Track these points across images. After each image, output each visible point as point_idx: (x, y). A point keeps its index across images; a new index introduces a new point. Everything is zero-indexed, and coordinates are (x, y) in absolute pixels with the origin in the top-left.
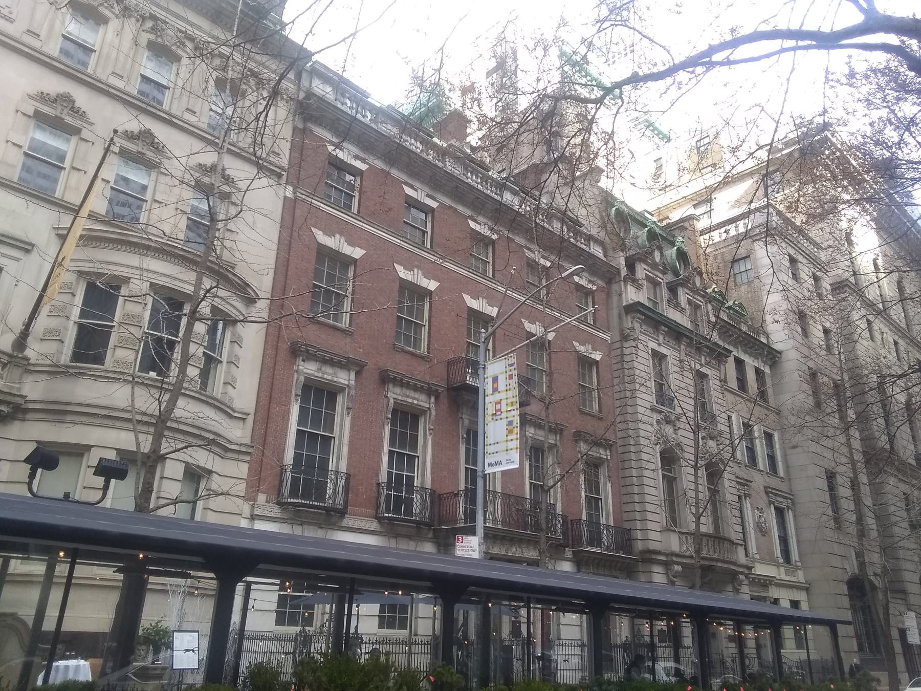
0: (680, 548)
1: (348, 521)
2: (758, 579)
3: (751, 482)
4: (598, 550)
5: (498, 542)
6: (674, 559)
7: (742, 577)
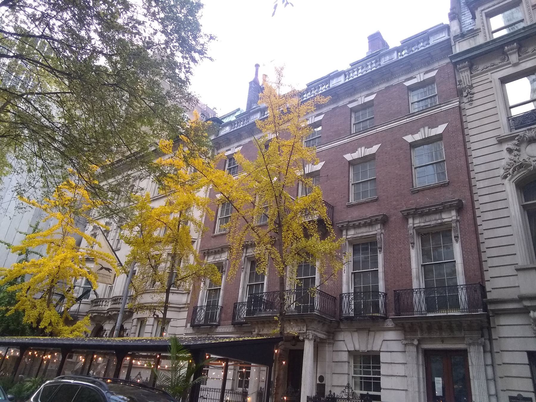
1: (220, 329)
5: (266, 325)
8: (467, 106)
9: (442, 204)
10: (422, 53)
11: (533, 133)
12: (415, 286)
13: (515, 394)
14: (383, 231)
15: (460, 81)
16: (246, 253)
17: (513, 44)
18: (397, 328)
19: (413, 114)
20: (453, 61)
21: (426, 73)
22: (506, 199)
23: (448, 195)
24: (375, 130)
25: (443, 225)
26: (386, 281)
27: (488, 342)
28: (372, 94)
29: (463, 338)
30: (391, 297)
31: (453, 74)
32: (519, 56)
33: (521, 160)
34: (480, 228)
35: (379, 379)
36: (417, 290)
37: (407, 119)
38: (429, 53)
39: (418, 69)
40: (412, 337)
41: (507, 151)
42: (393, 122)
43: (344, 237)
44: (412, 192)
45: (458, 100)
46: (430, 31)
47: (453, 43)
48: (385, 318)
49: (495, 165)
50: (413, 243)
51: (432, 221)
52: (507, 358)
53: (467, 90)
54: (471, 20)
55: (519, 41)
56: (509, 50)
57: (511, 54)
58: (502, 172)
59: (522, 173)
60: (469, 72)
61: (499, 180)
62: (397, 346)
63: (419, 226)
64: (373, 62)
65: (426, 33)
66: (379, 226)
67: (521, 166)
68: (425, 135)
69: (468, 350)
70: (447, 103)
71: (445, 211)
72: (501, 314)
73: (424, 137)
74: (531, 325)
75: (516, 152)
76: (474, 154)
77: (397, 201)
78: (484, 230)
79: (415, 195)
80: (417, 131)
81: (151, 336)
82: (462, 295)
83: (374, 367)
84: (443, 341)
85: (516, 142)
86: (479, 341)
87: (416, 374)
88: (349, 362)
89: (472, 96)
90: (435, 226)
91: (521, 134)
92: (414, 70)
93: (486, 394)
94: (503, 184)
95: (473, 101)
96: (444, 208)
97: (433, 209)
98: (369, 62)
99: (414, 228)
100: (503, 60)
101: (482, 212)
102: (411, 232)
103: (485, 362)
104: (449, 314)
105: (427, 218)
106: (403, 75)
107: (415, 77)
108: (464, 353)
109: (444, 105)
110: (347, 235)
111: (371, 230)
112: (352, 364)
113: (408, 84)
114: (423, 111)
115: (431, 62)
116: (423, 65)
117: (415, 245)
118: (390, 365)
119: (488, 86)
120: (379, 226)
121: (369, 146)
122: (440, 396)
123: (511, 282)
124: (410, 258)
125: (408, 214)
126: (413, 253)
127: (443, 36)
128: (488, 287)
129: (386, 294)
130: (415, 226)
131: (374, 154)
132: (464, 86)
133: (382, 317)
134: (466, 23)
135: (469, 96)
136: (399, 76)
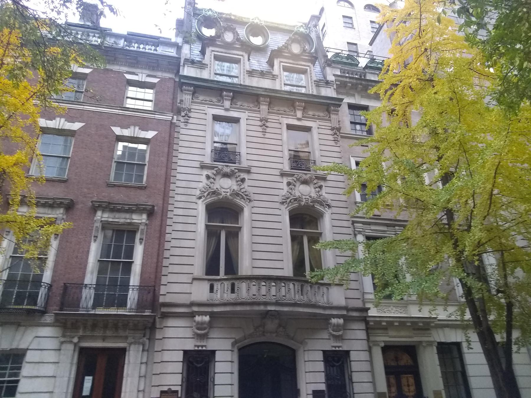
2: (412, 322)
3: (407, 221)
4: (121, 312)
6: (195, 309)
7: (334, 321)
8: (182, 125)
9: (136, 205)
10: (150, 55)
11: (229, 170)
12: (87, 281)
13: (165, 389)
14: (65, 217)
15: (182, 101)
17: (230, 93)
18: (56, 324)
19: (128, 109)
20: (182, 80)
21: (149, 76)
22: (196, 216)
23: (142, 198)
24: (82, 107)
25: (131, 225)
26: (55, 270)
27: (147, 341)
29: (126, 338)
30: (58, 291)
31: (172, 90)
32: (231, 104)
33: (215, 188)
34: (167, 236)
35: (17, 381)
36: (90, 286)
37: (120, 111)
38: (158, 60)
39: (142, 68)
40: (72, 334)
41: (206, 177)
42: (104, 107)
44: (108, 184)
45: (172, 115)
46: (161, 39)
47: (182, 64)
48: (43, 313)
49: (193, 185)
50: (97, 237)
51: (121, 218)
52: (167, 356)
53: (185, 112)
54: (198, 52)
55: (234, 92)
56: (226, 96)
57: (226, 99)
58: (198, 193)
59: (213, 198)
60: (191, 96)
61: (194, 199)
63: (107, 221)
64: (97, 35)
65: (157, 39)
66: (62, 210)
67: (214, 193)
68: (134, 135)
69: (128, 348)
70: (162, 113)
71: (137, 213)
72: (170, 317)
73: (132, 136)
74: (192, 327)
75: (212, 180)
76: (179, 169)
77: (89, 189)
78: (172, 239)
79: (110, 189)
80: (127, 127)
82: (132, 296)
83: (12, 369)
84: (104, 339)
85: (215, 172)
86: (141, 341)
87: (67, 374)
89: (188, 118)
90: (123, 224)
91: (220, 167)
92: (138, 68)
93: (136, 391)
94: (197, 203)
95: (188, 123)
96: (138, 209)
97: (127, 207)
98: (92, 32)
99: (101, 221)
100: (219, 101)
101: (174, 222)
102: (98, 225)
103: (141, 360)
104: (119, 313)
105: (117, 215)
106: (125, 65)
107: (137, 75)
108: (123, 352)
109: (158, 113)
111: (50, 212)
113: (129, 77)
114: (137, 111)
115: (156, 69)
116: (147, 67)
118: (37, 365)
119: (203, 116)
120: (62, 210)
121: (71, 119)
122: (87, 396)
123: (186, 288)
124: (88, 252)
125: (100, 206)
127: (171, 52)
128: (163, 290)
129: (50, 287)
130: (103, 219)
131: (75, 131)
132: (184, 107)
133: (42, 311)
134: (194, 52)
135: (186, 117)
136: (121, 65)
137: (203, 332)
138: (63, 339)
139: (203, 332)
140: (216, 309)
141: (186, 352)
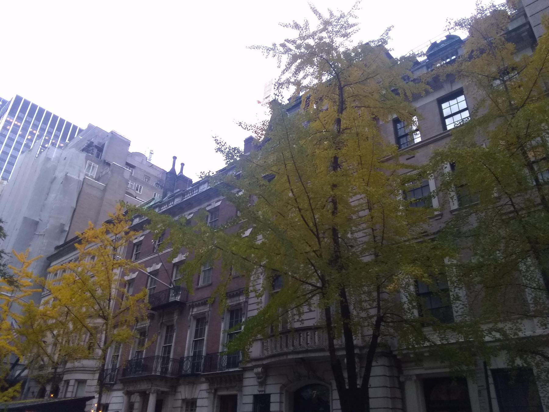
0: (263, 352)
6: (254, 363)
14: (211, 309)
16: (136, 326)
26: (207, 347)
28: (219, 201)
43: (190, 313)
50: (223, 318)
62: (205, 394)
81: (72, 394)
84: (228, 389)
88: (182, 407)
90: (236, 305)
97: (235, 293)
110: (192, 312)
112: (184, 408)
117: (225, 320)
126: (223, 325)
137: (260, 380)
138: (208, 391)
139: (260, 380)
140: (265, 362)
141: (255, 396)
